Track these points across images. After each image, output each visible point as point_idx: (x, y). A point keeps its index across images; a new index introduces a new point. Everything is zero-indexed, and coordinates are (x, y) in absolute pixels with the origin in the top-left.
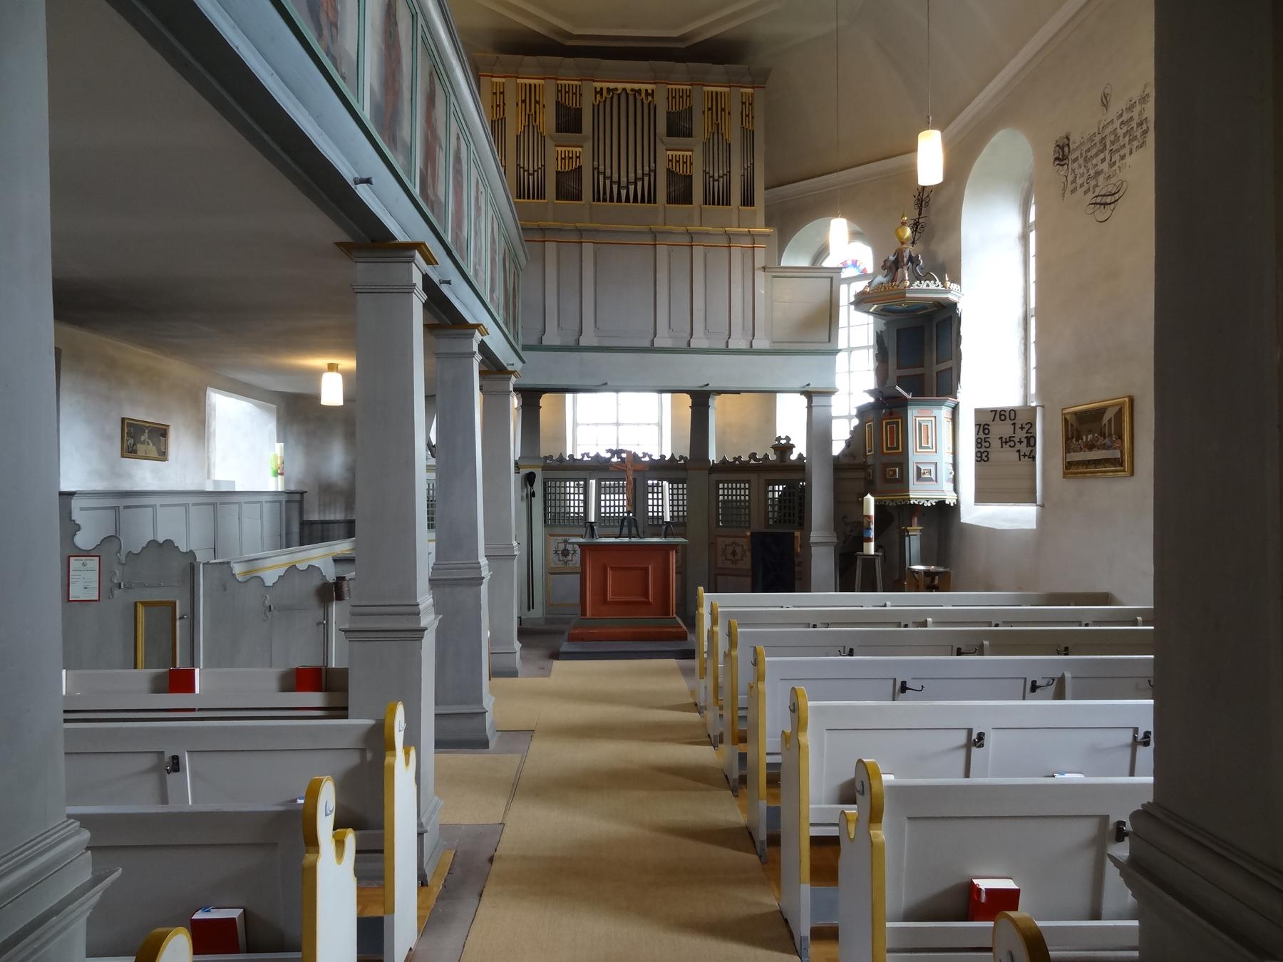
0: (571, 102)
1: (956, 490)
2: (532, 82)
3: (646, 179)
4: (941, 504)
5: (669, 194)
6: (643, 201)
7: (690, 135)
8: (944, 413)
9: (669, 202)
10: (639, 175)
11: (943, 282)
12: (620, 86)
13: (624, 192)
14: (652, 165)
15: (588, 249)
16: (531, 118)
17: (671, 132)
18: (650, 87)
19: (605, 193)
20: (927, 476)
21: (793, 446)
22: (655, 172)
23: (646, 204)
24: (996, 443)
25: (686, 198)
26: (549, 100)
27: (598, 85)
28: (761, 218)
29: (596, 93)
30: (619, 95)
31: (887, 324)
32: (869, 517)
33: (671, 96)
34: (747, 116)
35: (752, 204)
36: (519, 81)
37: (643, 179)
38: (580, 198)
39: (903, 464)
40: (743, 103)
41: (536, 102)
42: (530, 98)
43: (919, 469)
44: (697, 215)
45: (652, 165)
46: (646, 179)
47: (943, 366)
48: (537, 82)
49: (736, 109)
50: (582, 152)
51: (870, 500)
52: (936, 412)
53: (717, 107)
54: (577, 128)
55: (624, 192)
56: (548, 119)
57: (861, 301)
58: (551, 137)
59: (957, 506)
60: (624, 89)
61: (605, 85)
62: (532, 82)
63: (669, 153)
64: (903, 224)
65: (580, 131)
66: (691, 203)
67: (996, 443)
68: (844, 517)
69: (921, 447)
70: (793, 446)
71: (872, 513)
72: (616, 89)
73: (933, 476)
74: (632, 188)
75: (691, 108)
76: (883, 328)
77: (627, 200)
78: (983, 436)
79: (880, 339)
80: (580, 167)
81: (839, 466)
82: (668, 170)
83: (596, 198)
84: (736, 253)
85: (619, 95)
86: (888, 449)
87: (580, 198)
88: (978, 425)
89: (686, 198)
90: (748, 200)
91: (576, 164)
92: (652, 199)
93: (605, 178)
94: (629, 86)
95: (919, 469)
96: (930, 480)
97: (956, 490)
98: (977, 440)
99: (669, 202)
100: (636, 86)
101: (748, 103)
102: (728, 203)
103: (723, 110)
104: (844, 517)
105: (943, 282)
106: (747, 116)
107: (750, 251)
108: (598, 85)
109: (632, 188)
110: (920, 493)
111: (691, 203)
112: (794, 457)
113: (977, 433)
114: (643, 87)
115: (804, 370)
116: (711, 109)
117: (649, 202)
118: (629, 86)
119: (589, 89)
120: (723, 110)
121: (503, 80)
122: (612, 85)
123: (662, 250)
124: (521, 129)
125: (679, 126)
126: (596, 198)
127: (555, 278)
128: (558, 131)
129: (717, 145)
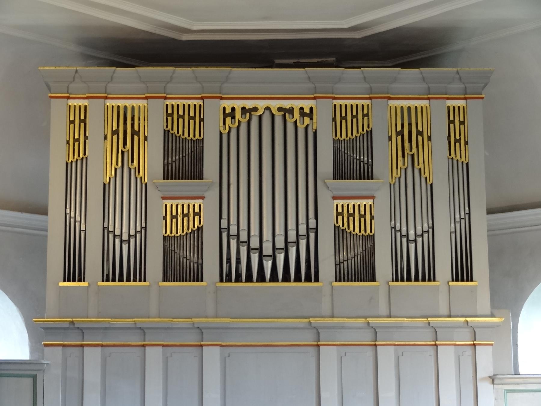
0: (186, 132)
2: (128, 103)
3: (303, 243)
5: (337, 265)
6: (298, 279)
7: (369, 176)
10: (292, 236)
12: (261, 104)
13: (268, 265)
14: (312, 225)
15: (212, 355)
16: (128, 156)
17: (340, 173)
18: (307, 105)
19: (238, 261)
23: (303, 284)
25: (367, 273)
26: (153, 129)
27: (228, 104)
28: (484, 301)
29: (225, 115)
30: (260, 117)
33: (339, 117)
34: (456, 142)
35: (470, 278)
36: (109, 103)
37: (297, 243)
38: (199, 278)
40: (450, 122)
46: (303, 243)
49: (439, 129)
50: (201, 204)
53: (409, 135)
54: (196, 172)
55: (268, 265)
56: (151, 158)
58: (157, 187)
60: (268, 109)
61: (238, 104)
62: (128, 103)
63: (340, 202)
65: (199, 176)
66: (373, 279)
72: (255, 109)
74: (281, 258)
75: (370, 133)
80: (200, 229)
82: (337, 228)
83: (226, 277)
84: (447, 355)
85: (260, 117)
87: (199, 278)
89: (367, 273)
90: (463, 272)
91: (193, 224)
92: (312, 276)
93: (239, 243)
94: (274, 104)
99: (339, 279)
100: (286, 104)
101: (455, 121)
102: (432, 278)
106: (456, 142)
107: (469, 351)
109: (281, 258)
111: (374, 280)
114: (296, 104)
118: (274, 104)
119: (213, 112)
120: (420, 133)
121: (85, 102)
122: (249, 104)
124: (109, 173)
125: (352, 166)
126: (226, 277)
127: (160, 396)
128: (166, 177)
129: (411, 185)
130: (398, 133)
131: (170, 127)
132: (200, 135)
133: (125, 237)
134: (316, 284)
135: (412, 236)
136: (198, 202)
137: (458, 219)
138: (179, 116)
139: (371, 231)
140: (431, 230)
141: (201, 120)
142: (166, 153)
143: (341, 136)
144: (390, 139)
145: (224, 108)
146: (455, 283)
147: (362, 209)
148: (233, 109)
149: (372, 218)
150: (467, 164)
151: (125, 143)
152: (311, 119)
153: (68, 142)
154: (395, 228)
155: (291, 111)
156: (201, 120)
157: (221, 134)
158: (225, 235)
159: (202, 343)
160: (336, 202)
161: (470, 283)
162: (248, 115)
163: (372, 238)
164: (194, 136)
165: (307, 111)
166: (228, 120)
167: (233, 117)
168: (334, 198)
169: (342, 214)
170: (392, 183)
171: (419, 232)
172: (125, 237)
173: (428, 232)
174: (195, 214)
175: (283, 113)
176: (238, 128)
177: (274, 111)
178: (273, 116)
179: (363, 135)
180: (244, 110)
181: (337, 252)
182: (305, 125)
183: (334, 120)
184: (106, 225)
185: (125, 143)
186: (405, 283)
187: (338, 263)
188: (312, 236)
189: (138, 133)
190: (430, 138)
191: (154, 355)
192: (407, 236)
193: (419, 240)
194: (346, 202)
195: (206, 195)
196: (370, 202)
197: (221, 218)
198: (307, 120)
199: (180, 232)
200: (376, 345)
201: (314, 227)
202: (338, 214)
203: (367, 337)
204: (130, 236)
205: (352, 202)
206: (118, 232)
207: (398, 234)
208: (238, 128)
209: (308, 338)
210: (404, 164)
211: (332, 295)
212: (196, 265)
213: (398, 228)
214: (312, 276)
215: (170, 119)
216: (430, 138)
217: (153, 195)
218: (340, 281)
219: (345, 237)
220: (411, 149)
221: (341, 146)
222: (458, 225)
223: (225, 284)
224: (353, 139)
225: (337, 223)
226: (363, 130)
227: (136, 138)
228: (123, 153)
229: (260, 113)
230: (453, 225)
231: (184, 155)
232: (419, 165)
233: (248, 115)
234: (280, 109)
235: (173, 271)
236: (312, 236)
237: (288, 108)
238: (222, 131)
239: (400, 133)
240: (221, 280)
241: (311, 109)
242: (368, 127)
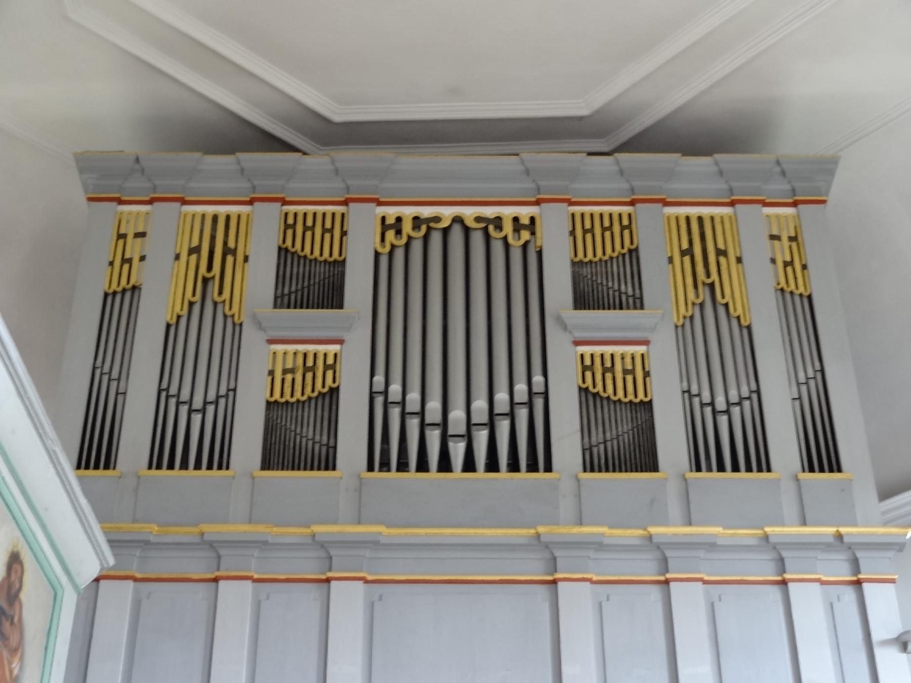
0: (316, 248)
3: (522, 414)
6: (514, 467)
7: (638, 303)
9: (590, 466)
13: (458, 450)
15: (348, 599)
17: (584, 299)
18: (525, 213)
22: (546, 395)
23: (523, 475)
27: (392, 212)
30: (446, 231)
33: (580, 230)
38: (329, 463)
41: (226, 251)
42: (215, 255)
44: (673, 491)
45: (538, 379)
46: (522, 414)
48: (233, 209)
55: (458, 450)
60: (458, 220)
61: (408, 212)
63: (587, 350)
66: (654, 467)
72: (437, 219)
74: (481, 438)
77: (469, 465)
80: (334, 392)
82: (583, 391)
83: (378, 460)
84: (808, 601)
85: (446, 231)
87: (329, 463)
90: (822, 455)
92: (539, 459)
94: (469, 213)
99: (590, 466)
100: (490, 212)
103: (721, 253)
107: (849, 594)
108: (392, 212)
116: (688, 252)
117: (533, 467)
122: (426, 212)
123: (576, 599)
126: (378, 460)
130: (683, 253)
131: (289, 243)
132: (340, 255)
133: (198, 403)
134: (548, 475)
135: (721, 404)
136: (333, 348)
137: (802, 379)
138: (305, 229)
139: (646, 395)
140: (755, 396)
141: (344, 233)
142: (281, 280)
143: (585, 256)
144: (671, 260)
145: (383, 219)
146: (808, 475)
147: (628, 360)
148: (399, 219)
149: (646, 374)
150: (810, 297)
151: (210, 268)
152: (533, 233)
153: (111, 264)
154: (689, 391)
155: (498, 222)
156: (344, 233)
157: (377, 255)
158: (379, 400)
159: (330, 575)
160: (581, 349)
161: (836, 476)
162: (424, 228)
163: (648, 406)
164: (331, 255)
165: (525, 221)
166: (390, 235)
167: (399, 232)
168: (577, 343)
169: (591, 367)
170: (680, 323)
171: (734, 398)
172: (198, 403)
173: (749, 398)
174: (326, 367)
175: (483, 225)
176: (407, 246)
177: (470, 223)
178: (467, 230)
179: (624, 255)
180: (417, 221)
181: (586, 429)
182: (522, 242)
183: (573, 233)
184: (164, 385)
185: (210, 268)
186: (715, 475)
187: (587, 446)
188: (539, 403)
189: (234, 252)
190: (739, 260)
191: (235, 597)
192: (712, 404)
193: (736, 411)
194: (598, 350)
195: (346, 336)
196: (642, 349)
197: (372, 374)
198: (525, 235)
199: (298, 395)
200: (667, 582)
201: (542, 390)
202: (585, 369)
203: (647, 569)
204: (206, 403)
205: (608, 350)
206: (185, 395)
207: (696, 400)
208: (407, 246)
209: (535, 569)
210: (697, 296)
211: (578, 496)
212: (324, 449)
213: (694, 390)
214: (539, 459)
215: (290, 232)
216: (739, 260)
217: (252, 339)
218: (592, 470)
219: (599, 406)
220: (708, 275)
221: (586, 271)
222: (804, 388)
223: (376, 474)
224: (606, 261)
225: (584, 382)
226: (623, 247)
227: (230, 259)
228: (206, 281)
229: (445, 224)
230: (795, 389)
231: (312, 282)
232: (723, 297)
233: (424, 228)
234: (478, 219)
235: (278, 454)
236: (539, 403)
237: (492, 217)
238: (380, 250)
239: (688, 252)
240: (370, 468)
241: (532, 219)
242: (632, 243)
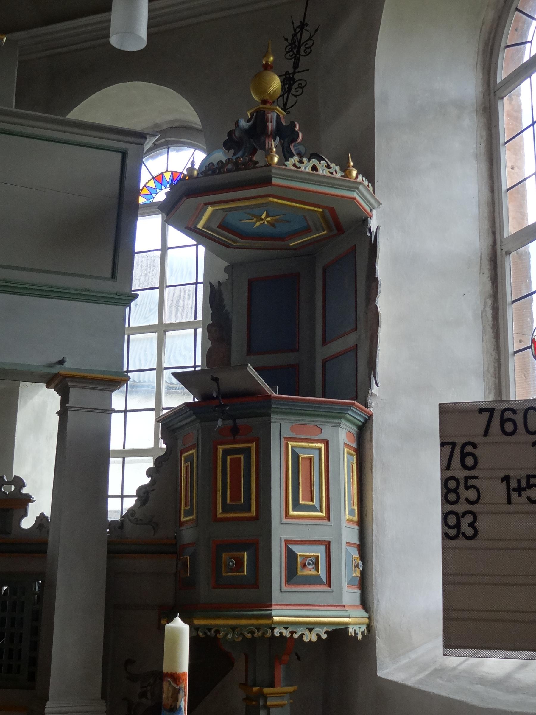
1: (365, 603)
4: (338, 634)
8: (342, 436)
11: (345, 169)
20: (310, 571)
21: (28, 499)
24: (493, 491)
31: (231, 269)
32: (176, 677)
39: (258, 544)
43: (292, 556)
47: (336, 347)
51: (180, 628)
52: (327, 432)
57: (184, 200)
59: (367, 643)
64: (267, 67)
67: (493, 491)
68: (129, 662)
69: (297, 506)
70: (28, 499)
71: (184, 666)
73: (322, 573)
76: (223, 277)
78: (461, 474)
79: (215, 297)
81: (125, 544)
86: (226, 508)
88: (442, 445)
95: (292, 556)
96: (315, 580)
97: (365, 603)
98: (445, 483)
104: (129, 662)
105: (345, 169)
110: (296, 612)
112: (27, 523)
113: (446, 466)
115: (54, 328)
